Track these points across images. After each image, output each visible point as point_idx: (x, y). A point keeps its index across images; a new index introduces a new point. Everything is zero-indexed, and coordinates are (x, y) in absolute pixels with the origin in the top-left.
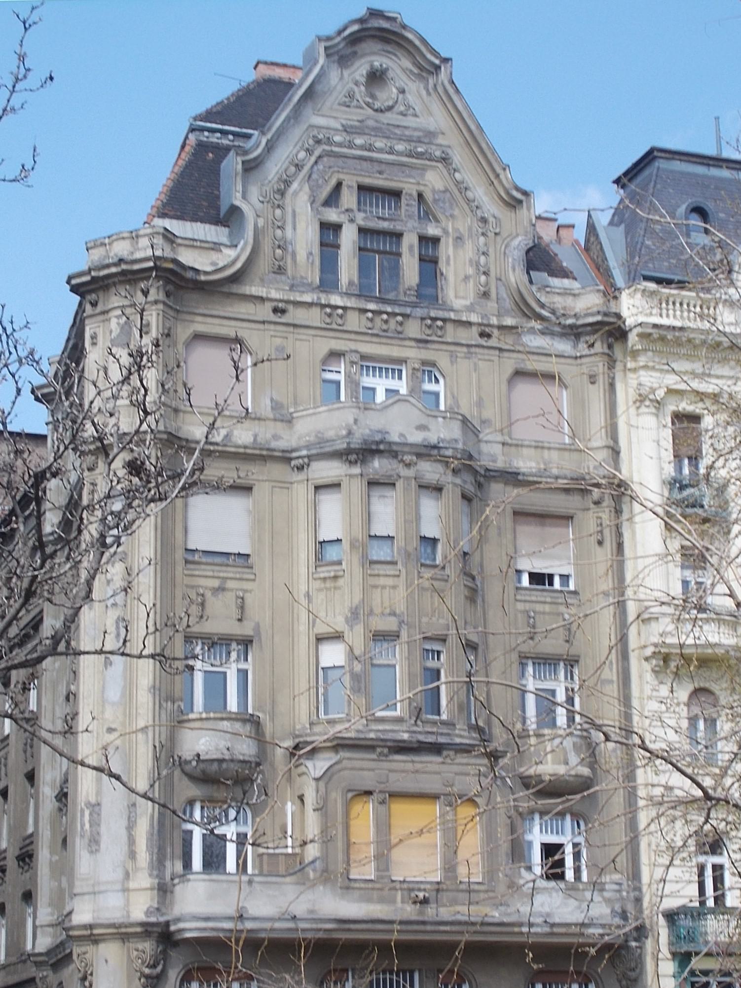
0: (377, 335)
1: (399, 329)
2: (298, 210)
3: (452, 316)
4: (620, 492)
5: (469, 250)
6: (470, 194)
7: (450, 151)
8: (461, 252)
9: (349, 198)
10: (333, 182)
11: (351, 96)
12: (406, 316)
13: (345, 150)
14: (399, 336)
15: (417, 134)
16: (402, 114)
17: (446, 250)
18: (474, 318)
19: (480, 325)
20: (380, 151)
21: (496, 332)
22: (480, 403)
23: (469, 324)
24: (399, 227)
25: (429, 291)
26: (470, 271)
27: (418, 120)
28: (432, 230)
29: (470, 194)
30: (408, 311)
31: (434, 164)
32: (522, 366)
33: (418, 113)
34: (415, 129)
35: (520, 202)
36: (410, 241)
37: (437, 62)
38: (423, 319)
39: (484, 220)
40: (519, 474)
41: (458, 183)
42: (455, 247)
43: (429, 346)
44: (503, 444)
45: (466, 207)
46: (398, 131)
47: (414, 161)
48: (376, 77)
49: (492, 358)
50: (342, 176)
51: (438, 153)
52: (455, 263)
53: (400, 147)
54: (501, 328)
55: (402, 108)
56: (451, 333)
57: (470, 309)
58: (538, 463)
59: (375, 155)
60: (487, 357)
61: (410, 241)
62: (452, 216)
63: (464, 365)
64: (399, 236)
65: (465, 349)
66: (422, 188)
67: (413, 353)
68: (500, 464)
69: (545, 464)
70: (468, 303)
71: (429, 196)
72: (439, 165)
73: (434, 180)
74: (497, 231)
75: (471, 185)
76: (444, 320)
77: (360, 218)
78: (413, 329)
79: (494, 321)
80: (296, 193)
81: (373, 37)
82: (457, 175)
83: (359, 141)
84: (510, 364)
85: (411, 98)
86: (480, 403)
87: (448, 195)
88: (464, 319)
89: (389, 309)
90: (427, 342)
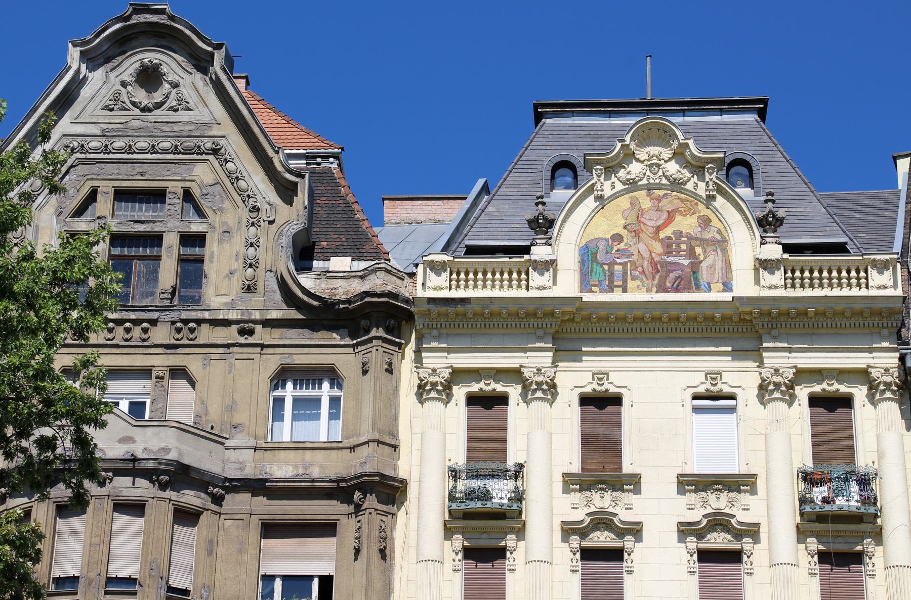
0: (117, 346)
1: (144, 336)
2: (41, 225)
3: (207, 315)
4: (390, 491)
5: (237, 243)
6: (242, 184)
7: (222, 142)
8: (227, 246)
9: (103, 205)
10: (85, 190)
11: (116, 98)
12: (154, 322)
13: (149, 156)
14: (145, 344)
15: (187, 128)
16: (172, 109)
17: (212, 246)
18: (233, 315)
19: (237, 322)
20: (143, 151)
21: (258, 328)
22: (231, 407)
23: (226, 323)
24: (157, 228)
25: (192, 292)
26: (238, 265)
27: (191, 113)
28: (197, 226)
29: (242, 184)
30: (155, 315)
31: (204, 157)
32: (289, 361)
33: (192, 105)
34: (187, 123)
35: (296, 184)
36: (171, 240)
37: (210, 49)
38: (173, 323)
39: (255, 209)
40: (266, 480)
41: (229, 174)
42: (221, 241)
43: (179, 351)
44: (255, 449)
45: (238, 199)
46: (166, 128)
47: (181, 156)
48: (149, 77)
49: (251, 356)
50: (96, 183)
51: (209, 145)
52: (222, 262)
53: (166, 145)
54: (268, 323)
55: (174, 103)
56: (205, 334)
57: (232, 306)
58: (296, 467)
59: (135, 156)
60: (245, 356)
61: (171, 240)
62: (220, 209)
63: (218, 367)
64: (156, 239)
65: (221, 350)
66: (188, 184)
67: (160, 361)
68: (249, 472)
69: (305, 468)
70: (228, 299)
71: (196, 192)
72: (211, 157)
73: (203, 174)
74: (271, 219)
75: (245, 174)
76: (199, 322)
77: (114, 225)
78: (161, 334)
79: (257, 316)
80: (41, 207)
81: (145, 33)
82: (229, 165)
83: (119, 144)
84: (272, 362)
85: (187, 92)
86: (231, 407)
87: (218, 187)
88: (221, 317)
89: (133, 316)
90: (176, 347)
